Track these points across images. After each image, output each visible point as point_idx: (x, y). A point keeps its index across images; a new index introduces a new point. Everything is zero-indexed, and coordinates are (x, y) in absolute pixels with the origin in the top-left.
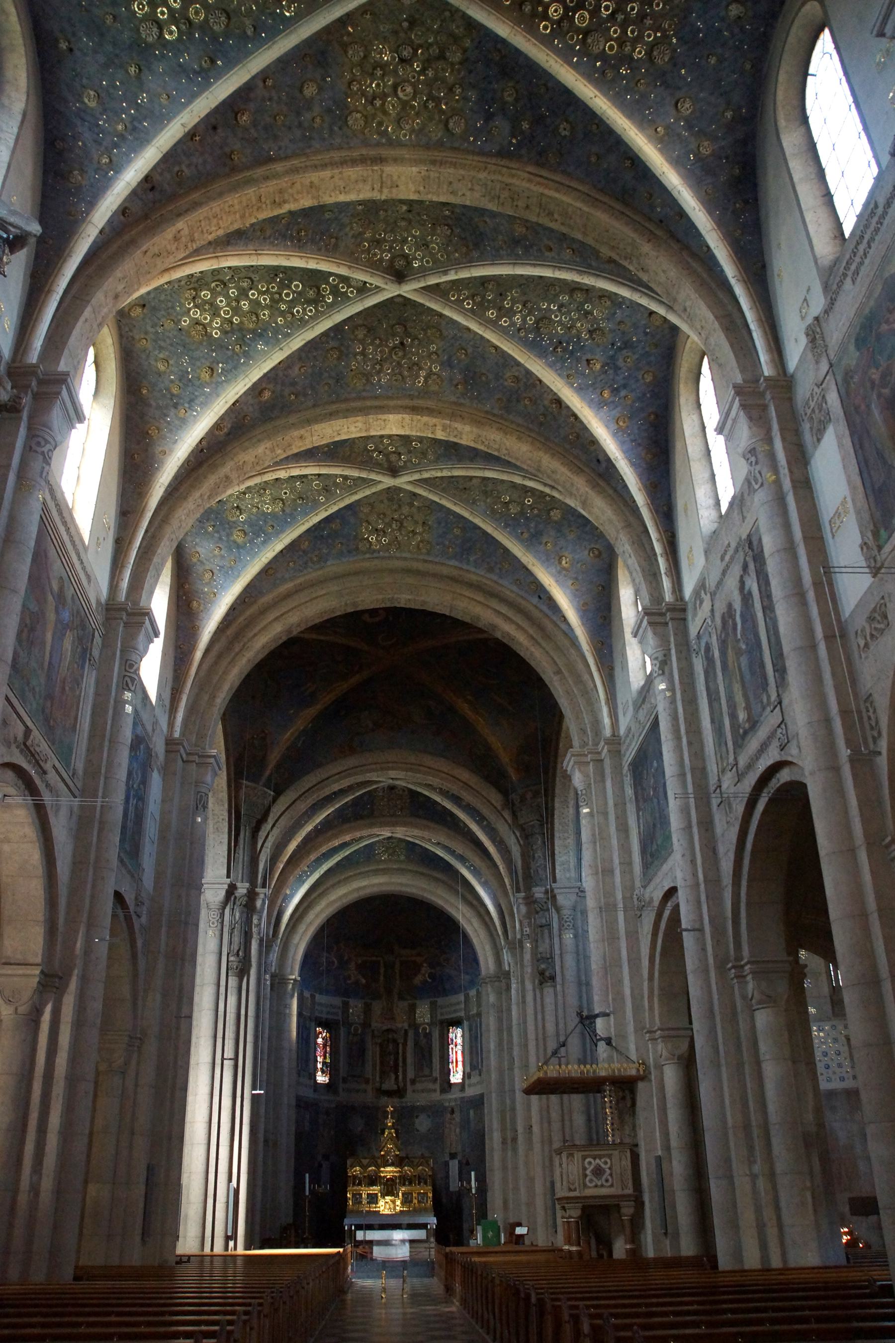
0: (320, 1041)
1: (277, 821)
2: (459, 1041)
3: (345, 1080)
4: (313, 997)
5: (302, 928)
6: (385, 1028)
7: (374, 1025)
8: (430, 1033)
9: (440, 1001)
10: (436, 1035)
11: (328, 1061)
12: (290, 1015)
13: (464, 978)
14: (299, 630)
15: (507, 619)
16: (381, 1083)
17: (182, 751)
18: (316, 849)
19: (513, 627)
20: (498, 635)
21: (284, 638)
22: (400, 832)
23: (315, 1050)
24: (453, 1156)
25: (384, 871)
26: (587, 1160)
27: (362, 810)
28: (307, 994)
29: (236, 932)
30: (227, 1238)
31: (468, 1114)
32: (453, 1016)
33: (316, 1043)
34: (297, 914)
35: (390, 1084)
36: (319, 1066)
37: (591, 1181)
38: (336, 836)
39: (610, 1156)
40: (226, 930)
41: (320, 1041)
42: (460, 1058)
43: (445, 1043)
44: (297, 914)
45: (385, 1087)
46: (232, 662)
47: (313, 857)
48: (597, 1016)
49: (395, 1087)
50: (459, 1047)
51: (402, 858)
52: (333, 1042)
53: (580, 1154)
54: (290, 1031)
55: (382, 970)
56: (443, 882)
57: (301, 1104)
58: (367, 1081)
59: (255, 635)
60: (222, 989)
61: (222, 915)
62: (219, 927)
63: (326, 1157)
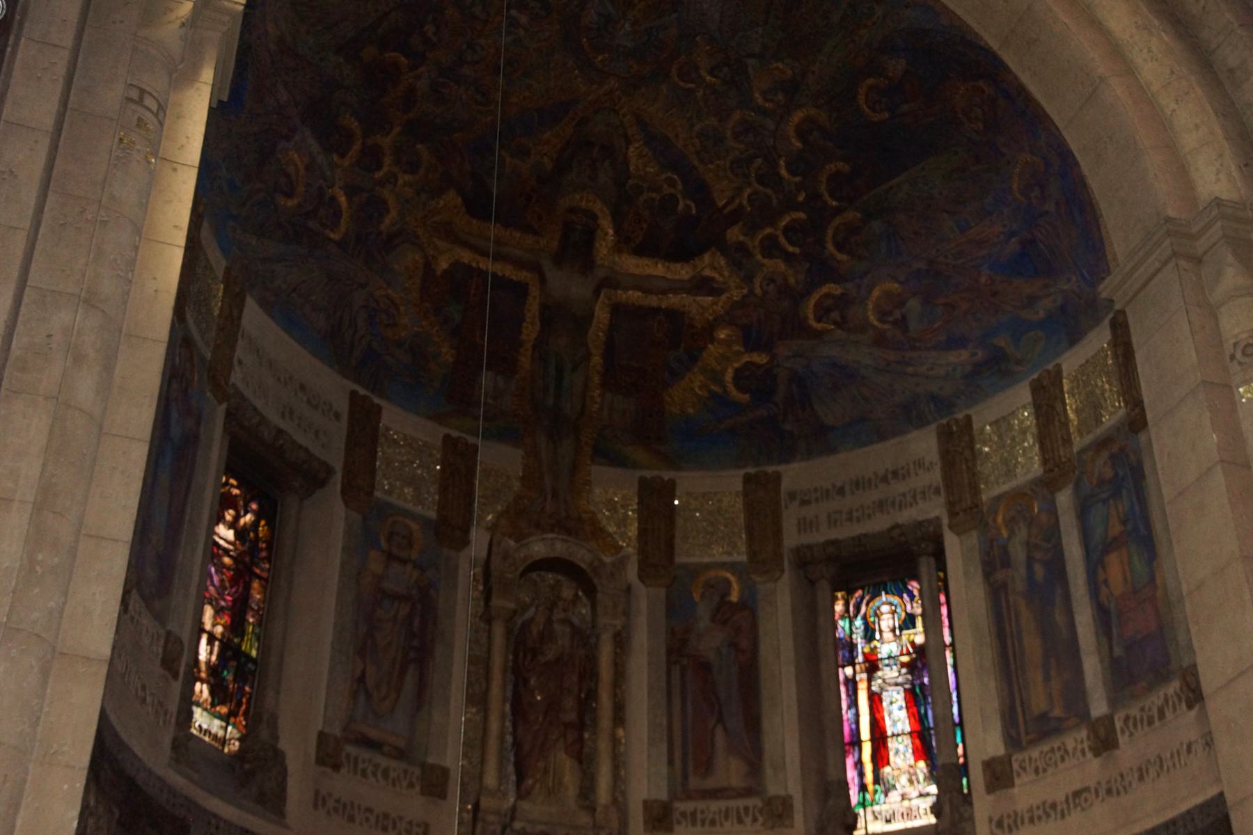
6: (539, 548)
8: (748, 606)
9: (794, 475)
32: (879, 524)
42: (897, 718)
43: (822, 656)
54: (141, 230)
55: (530, 331)
58: (434, 784)
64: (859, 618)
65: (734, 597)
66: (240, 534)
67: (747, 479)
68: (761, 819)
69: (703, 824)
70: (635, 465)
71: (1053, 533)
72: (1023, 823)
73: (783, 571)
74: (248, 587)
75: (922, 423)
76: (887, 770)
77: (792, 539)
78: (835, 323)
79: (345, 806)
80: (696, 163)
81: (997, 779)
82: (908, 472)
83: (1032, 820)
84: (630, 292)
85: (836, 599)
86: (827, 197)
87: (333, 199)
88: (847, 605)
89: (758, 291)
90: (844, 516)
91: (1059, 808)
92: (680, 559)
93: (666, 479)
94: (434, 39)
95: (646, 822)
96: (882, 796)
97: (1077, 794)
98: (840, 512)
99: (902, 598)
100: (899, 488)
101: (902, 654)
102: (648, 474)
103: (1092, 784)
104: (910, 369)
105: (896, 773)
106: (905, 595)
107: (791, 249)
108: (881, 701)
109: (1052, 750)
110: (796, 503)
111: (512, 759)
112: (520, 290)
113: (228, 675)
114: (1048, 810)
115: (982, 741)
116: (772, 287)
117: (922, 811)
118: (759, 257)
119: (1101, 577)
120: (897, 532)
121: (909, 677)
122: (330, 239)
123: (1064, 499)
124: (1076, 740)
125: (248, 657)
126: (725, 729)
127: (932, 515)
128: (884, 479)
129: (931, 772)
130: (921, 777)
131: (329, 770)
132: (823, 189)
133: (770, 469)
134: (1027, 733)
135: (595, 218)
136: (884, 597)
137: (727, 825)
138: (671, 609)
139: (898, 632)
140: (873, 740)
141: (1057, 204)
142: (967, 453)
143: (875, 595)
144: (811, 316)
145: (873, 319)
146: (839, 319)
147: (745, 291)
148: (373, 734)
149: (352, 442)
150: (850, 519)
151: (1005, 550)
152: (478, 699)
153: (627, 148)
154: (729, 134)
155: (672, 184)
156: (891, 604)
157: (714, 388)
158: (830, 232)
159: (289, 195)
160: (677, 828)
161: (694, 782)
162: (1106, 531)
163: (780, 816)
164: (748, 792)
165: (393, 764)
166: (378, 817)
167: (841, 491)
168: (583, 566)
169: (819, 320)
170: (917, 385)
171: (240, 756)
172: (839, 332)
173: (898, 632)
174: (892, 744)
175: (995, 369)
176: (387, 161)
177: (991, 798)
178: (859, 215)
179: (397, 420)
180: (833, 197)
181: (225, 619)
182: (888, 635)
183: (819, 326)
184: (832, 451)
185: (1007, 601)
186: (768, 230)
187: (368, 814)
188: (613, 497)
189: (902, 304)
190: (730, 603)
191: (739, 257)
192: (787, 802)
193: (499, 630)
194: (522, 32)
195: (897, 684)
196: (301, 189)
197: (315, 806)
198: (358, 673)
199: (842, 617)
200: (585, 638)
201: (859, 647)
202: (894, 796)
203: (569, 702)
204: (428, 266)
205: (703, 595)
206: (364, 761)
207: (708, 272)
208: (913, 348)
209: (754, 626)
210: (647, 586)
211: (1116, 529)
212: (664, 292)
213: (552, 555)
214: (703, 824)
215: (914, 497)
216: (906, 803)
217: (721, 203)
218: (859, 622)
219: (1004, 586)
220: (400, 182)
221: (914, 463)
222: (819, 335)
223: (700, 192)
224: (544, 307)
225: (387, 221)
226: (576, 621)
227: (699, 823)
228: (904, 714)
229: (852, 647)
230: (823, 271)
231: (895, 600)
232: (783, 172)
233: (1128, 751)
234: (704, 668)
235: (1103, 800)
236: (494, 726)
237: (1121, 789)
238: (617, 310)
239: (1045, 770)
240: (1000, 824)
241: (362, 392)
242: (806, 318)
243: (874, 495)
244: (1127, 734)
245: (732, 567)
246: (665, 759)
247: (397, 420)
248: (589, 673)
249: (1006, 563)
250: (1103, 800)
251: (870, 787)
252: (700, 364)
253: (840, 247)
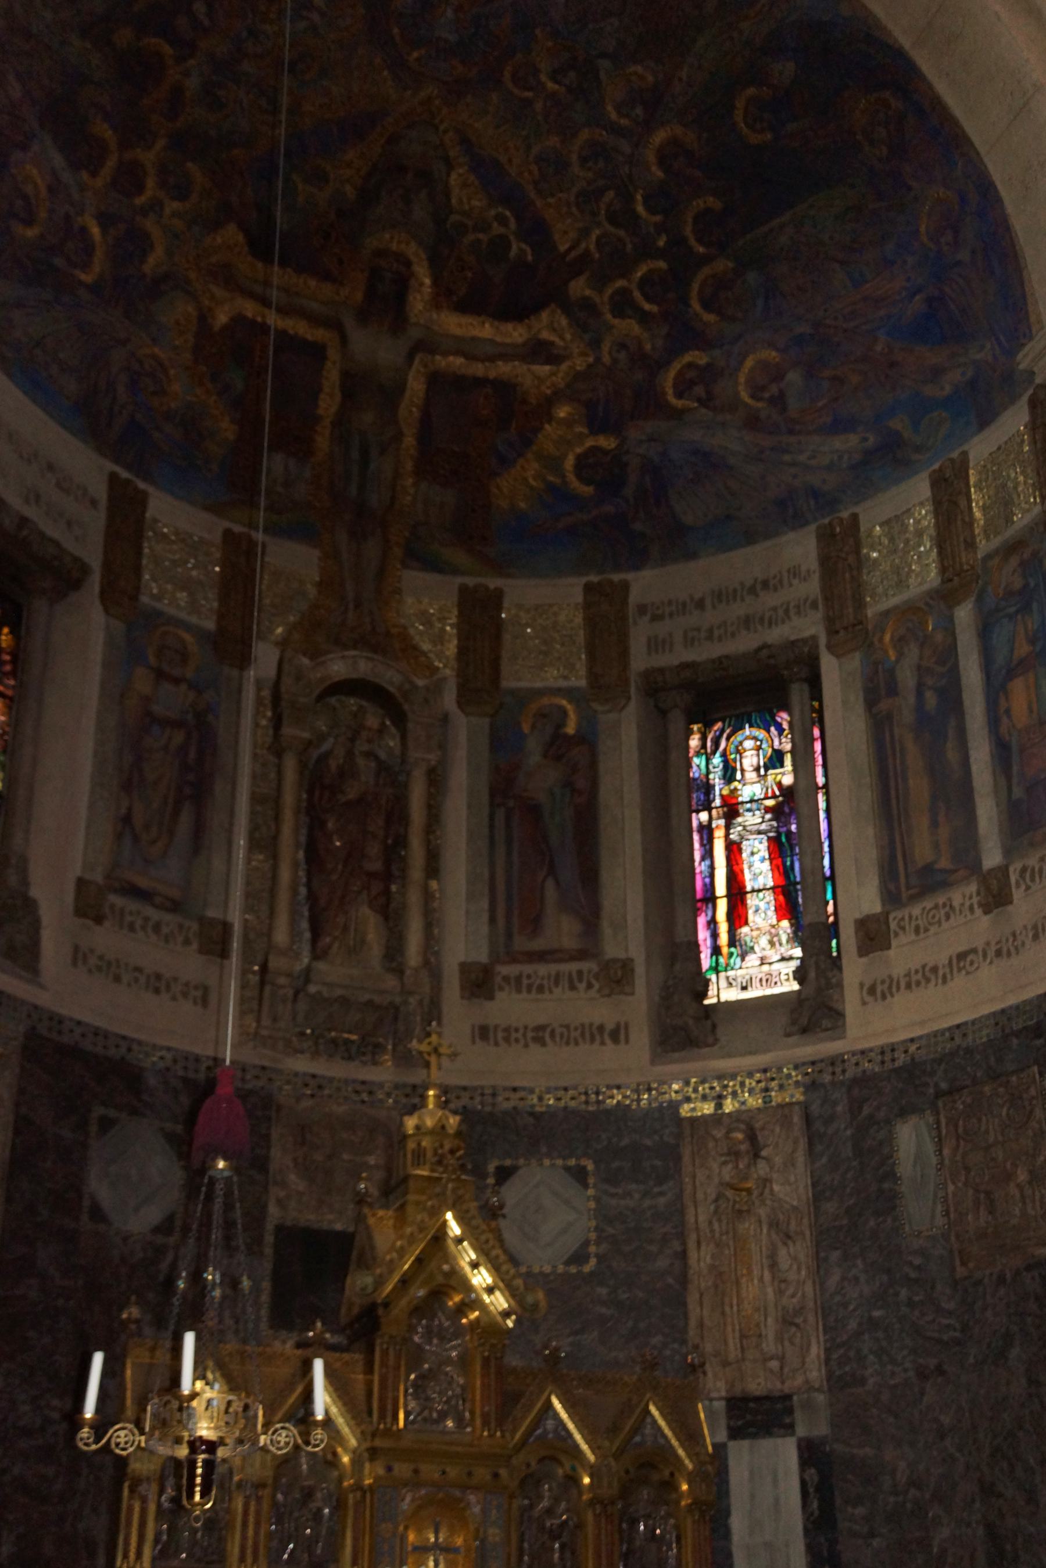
8: (587, 740)
9: (646, 584)
24: (756, 1416)
32: (744, 643)
42: (759, 870)
43: (673, 800)
55: (328, 404)
58: (215, 942)
64: (718, 754)
65: (570, 729)
67: (588, 588)
68: (597, 986)
69: (529, 991)
70: (455, 571)
71: (949, 654)
72: (898, 989)
73: (629, 698)
75: (798, 521)
76: (745, 930)
77: (640, 660)
78: (699, 400)
79: (109, 963)
80: (533, 195)
81: (872, 939)
82: (781, 582)
83: (909, 986)
84: (451, 358)
85: (692, 732)
86: (692, 242)
87: (84, 230)
88: (703, 739)
89: (606, 359)
90: (703, 634)
91: (941, 973)
92: (508, 683)
93: (492, 586)
94: (206, 22)
95: (463, 988)
96: (739, 960)
97: (962, 956)
98: (698, 630)
99: (768, 731)
100: (770, 600)
101: (766, 798)
102: (470, 581)
103: (980, 944)
104: (787, 458)
105: (755, 933)
106: (772, 729)
107: (647, 307)
108: (740, 851)
109: (936, 907)
110: (647, 618)
111: (306, 914)
112: (318, 352)
114: (928, 974)
115: (857, 897)
116: (622, 356)
117: (783, 977)
118: (609, 316)
119: (1003, 704)
120: (765, 653)
121: (775, 823)
122: (81, 283)
123: (964, 614)
124: (964, 896)
126: (558, 883)
127: (806, 634)
128: (752, 591)
129: (795, 933)
130: (784, 938)
131: (90, 923)
132: (688, 231)
133: (616, 577)
134: (908, 888)
135: (408, 264)
136: (747, 731)
137: (558, 991)
138: (496, 743)
139: (762, 772)
140: (729, 896)
141: (973, 252)
142: (851, 559)
143: (738, 728)
144: (670, 391)
145: (744, 396)
146: (703, 395)
147: (591, 360)
148: (143, 883)
149: (113, 535)
150: (710, 637)
151: (891, 673)
152: (264, 842)
153: (448, 175)
154: (574, 157)
155: (502, 221)
156: (755, 739)
157: (551, 478)
158: (696, 286)
159: (29, 222)
160: (500, 996)
161: (522, 943)
162: (1012, 651)
163: (618, 982)
164: (582, 955)
165: (168, 917)
166: (148, 977)
167: (700, 605)
168: (391, 689)
169: (679, 395)
170: (795, 476)
172: (704, 411)
173: (762, 772)
174: (752, 901)
175: (890, 457)
176: (150, 183)
177: (864, 960)
178: (731, 265)
179: (167, 511)
180: (700, 241)
182: (751, 776)
183: (678, 403)
184: (691, 555)
185: (892, 736)
186: (620, 283)
187: (136, 974)
188: (427, 608)
189: (778, 376)
190: (566, 735)
191: (583, 315)
192: (627, 965)
193: (290, 764)
194: (315, 17)
195: (759, 832)
196: (43, 215)
197: (75, 963)
198: (123, 811)
199: (698, 754)
200: (393, 776)
201: (717, 788)
202: (752, 960)
203: (374, 849)
204: (203, 319)
205: (533, 727)
206: (131, 913)
207: (545, 335)
208: (791, 432)
209: (593, 764)
210: (467, 714)
211: (1023, 649)
212: (492, 359)
213: (354, 676)
214: (529, 991)
215: (787, 611)
216: (765, 968)
217: (563, 248)
218: (717, 760)
219: (889, 717)
220: (167, 211)
221: (789, 571)
222: (677, 415)
223: (537, 232)
224: (346, 375)
225: (151, 260)
226: (383, 755)
227: (524, 990)
228: (766, 866)
229: (709, 788)
230: (686, 335)
231: (761, 734)
232: (640, 209)
233: (1024, 908)
234: (533, 811)
235: (991, 963)
236: (285, 875)
237: (1012, 949)
238: (435, 380)
239: (926, 930)
240: (872, 991)
241: (125, 474)
242: (664, 394)
243: (738, 610)
244: (1023, 887)
246: (485, 917)
247: (167, 511)
248: (397, 815)
249: (893, 690)
250: (991, 963)
251: (725, 950)
252: (535, 448)
253: (707, 306)
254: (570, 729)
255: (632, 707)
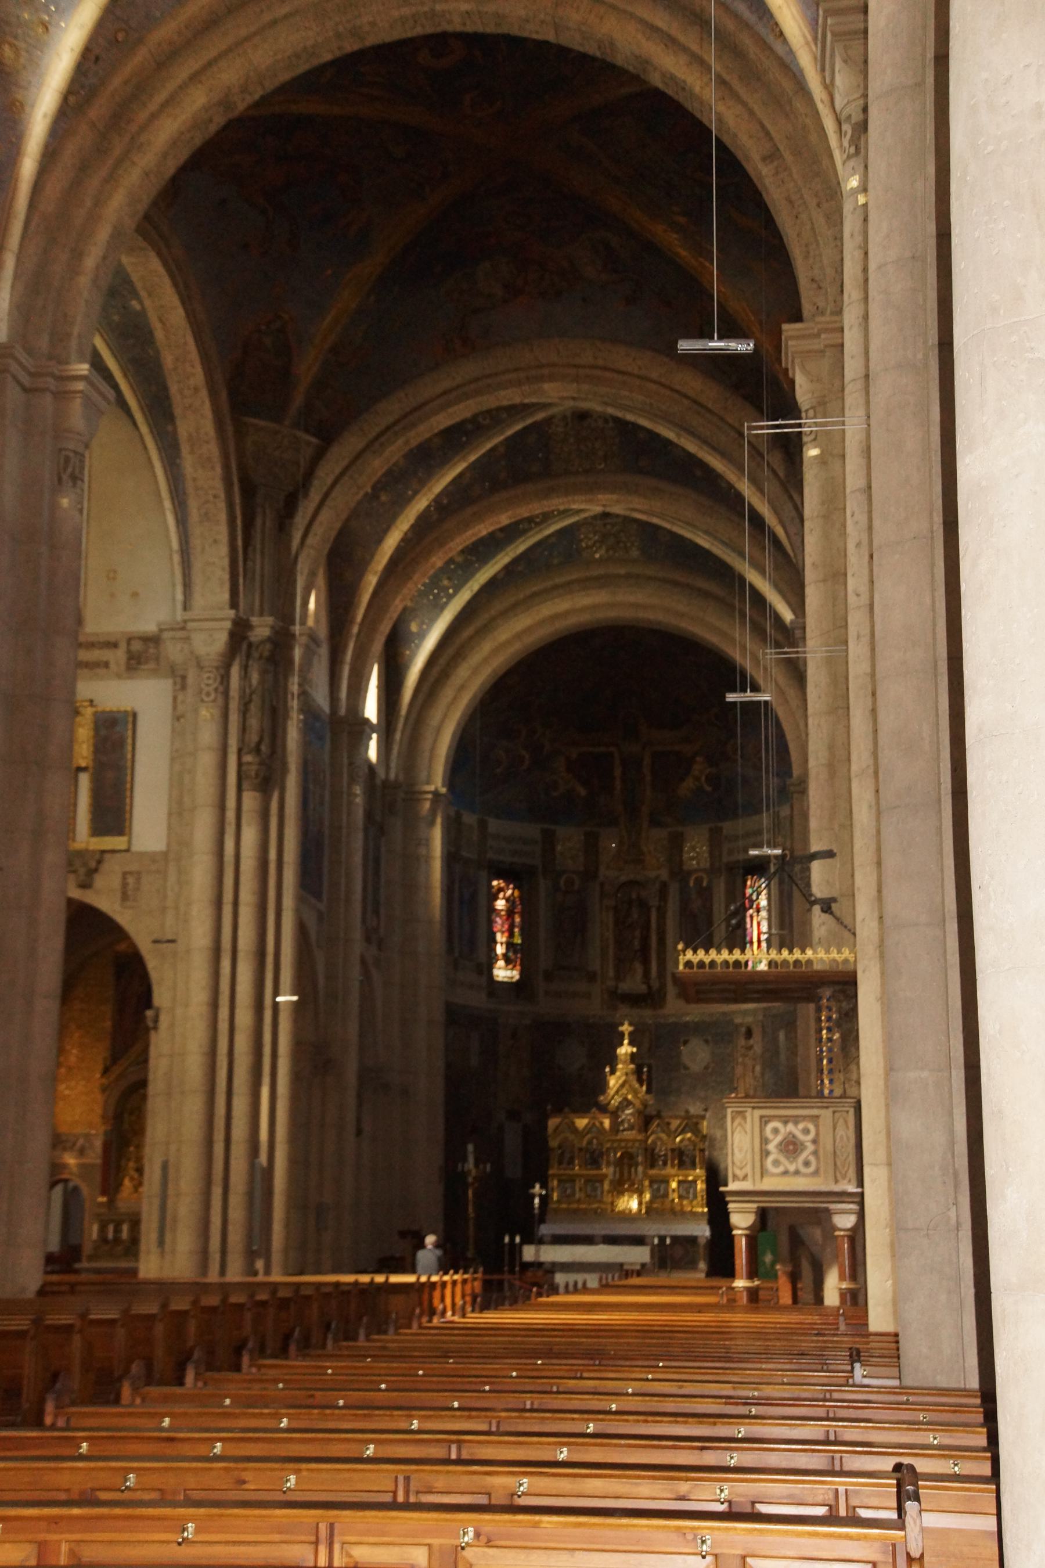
0: (500, 904)
1: (326, 495)
2: (763, 902)
3: (548, 976)
4: (483, 824)
5: (448, 693)
6: (623, 879)
7: (603, 871)
8: (709, 888)
9: (728, 827)
10: (720, 889)
11: (518, 940)
12: (428, 858)
13: (769, 784)
14: (249, 100)
15: (671, 42)
16: (618, 978)
17: (14, 367)
18: (442, 545)
19: (683, 59)
20: (656, 80)
21: (220, 120)
22: (618, 505)
23: (490, 923)
25: (603, 582)
26: (770, 1126)
27: (532, 459)
28: (470, 819)
29: (253, 708)
30: (251, 1255)
31: (775, 1040)
33: (492, 910)
34: (435, 671)
35: (633, 984)
36: (500, 950)
37: (776, 1163)
38: (478, 518)
39: (815, 1119)
40: (234, 705)
41: (500, 904)
44: (435, 671)
45: (625, 987)
46: (111, 179)
47: (438, 561)
48: (814, 856)
49: (643, 988)
50: (764, 914)
51: (635, 553)
52: (525, 907)
53: (758, 1113)
54: (428, 887)
55: (618, 772)
56: (717, 599)
57: (456, 1017)
58: (592, 977)
59: (154, 116)
60: (231, 815)
61: (225, 678)
62: (220, 700)
63: (514, 1115)
65: (705, 884)
66: (507, 900)
67: (711, 830)
74: (513, 919)
92: (685, 867)
113: (510, 954)
125: (517, 944)
133: (720, 824)
171: (518, 981)
181: (506, 934)
241: (546, 826)
245: (704, 870)
254: (705, 884)
255: (723, 878)
